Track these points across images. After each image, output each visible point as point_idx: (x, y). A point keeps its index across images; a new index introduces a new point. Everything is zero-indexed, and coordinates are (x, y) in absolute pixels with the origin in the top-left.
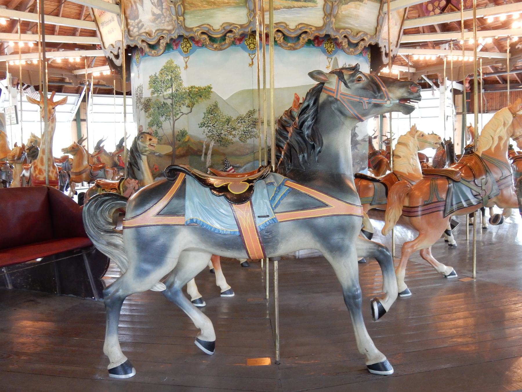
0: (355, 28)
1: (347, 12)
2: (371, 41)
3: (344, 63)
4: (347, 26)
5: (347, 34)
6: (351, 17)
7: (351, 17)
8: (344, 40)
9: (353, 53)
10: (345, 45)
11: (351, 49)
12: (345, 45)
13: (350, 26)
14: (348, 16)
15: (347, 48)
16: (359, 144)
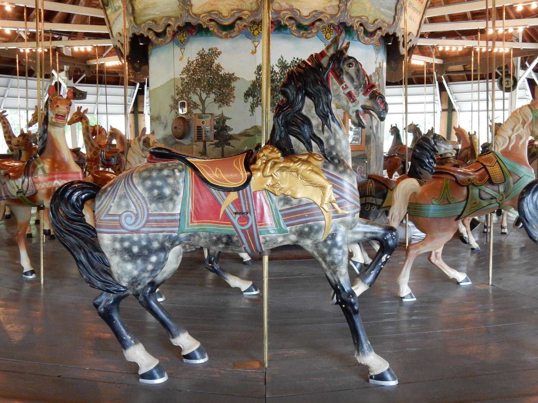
0: (157, 16)
1: (143, 4)
2: (179, 23)
3: (201, 49)
4: (148, 18)
5: (150, 26)
6: (149, 8)
7: (149, 8)
8: (149, 33)
9: (164, 42)
10: (152, 38)
11: (160, 40)
12: (152, 38)
13: (151, 17)
14: (145, 8)
15: (155, 39)
16: (234, 139)
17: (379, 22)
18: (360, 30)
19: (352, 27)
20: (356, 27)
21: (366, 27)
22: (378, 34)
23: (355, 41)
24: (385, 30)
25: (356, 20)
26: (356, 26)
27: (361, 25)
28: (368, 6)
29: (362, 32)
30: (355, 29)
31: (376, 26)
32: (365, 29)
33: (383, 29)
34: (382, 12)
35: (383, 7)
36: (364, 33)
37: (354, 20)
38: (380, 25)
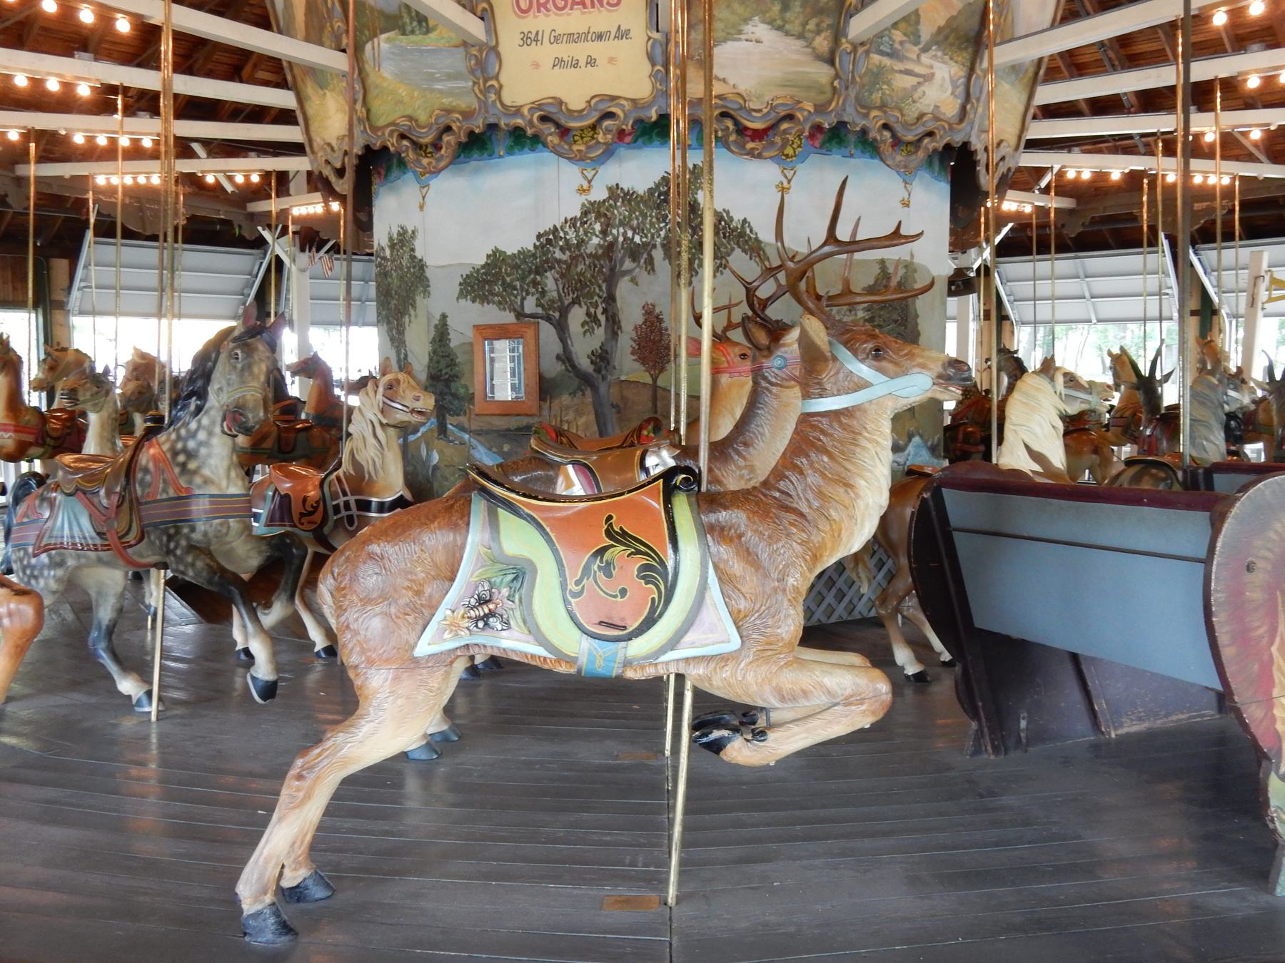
17: (438, 117)
18: (404, 148)
19: (385, 149)
20: (393, 145)
21: (414, 138)
22: (448, 143)
23: (501, 157)
24: (460, 128)
25: (387, 131)
26: (392, 143)
27: (403, 136)
28: (403, 92)
29: (410, 151)
30: (392, 149)
31: (435, 127)
32: (414, 143)
33: (454, 128)
34: (441, 91)
35: (439, 80)
36: (414, 150)
37: (383, 134)
38: (444, 121)
